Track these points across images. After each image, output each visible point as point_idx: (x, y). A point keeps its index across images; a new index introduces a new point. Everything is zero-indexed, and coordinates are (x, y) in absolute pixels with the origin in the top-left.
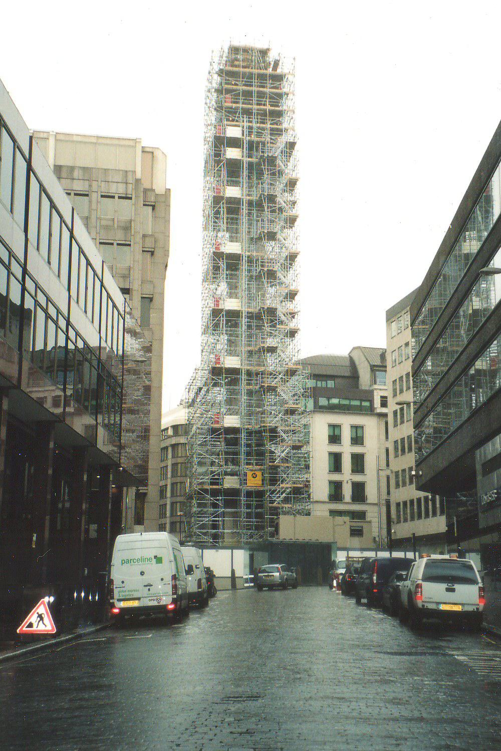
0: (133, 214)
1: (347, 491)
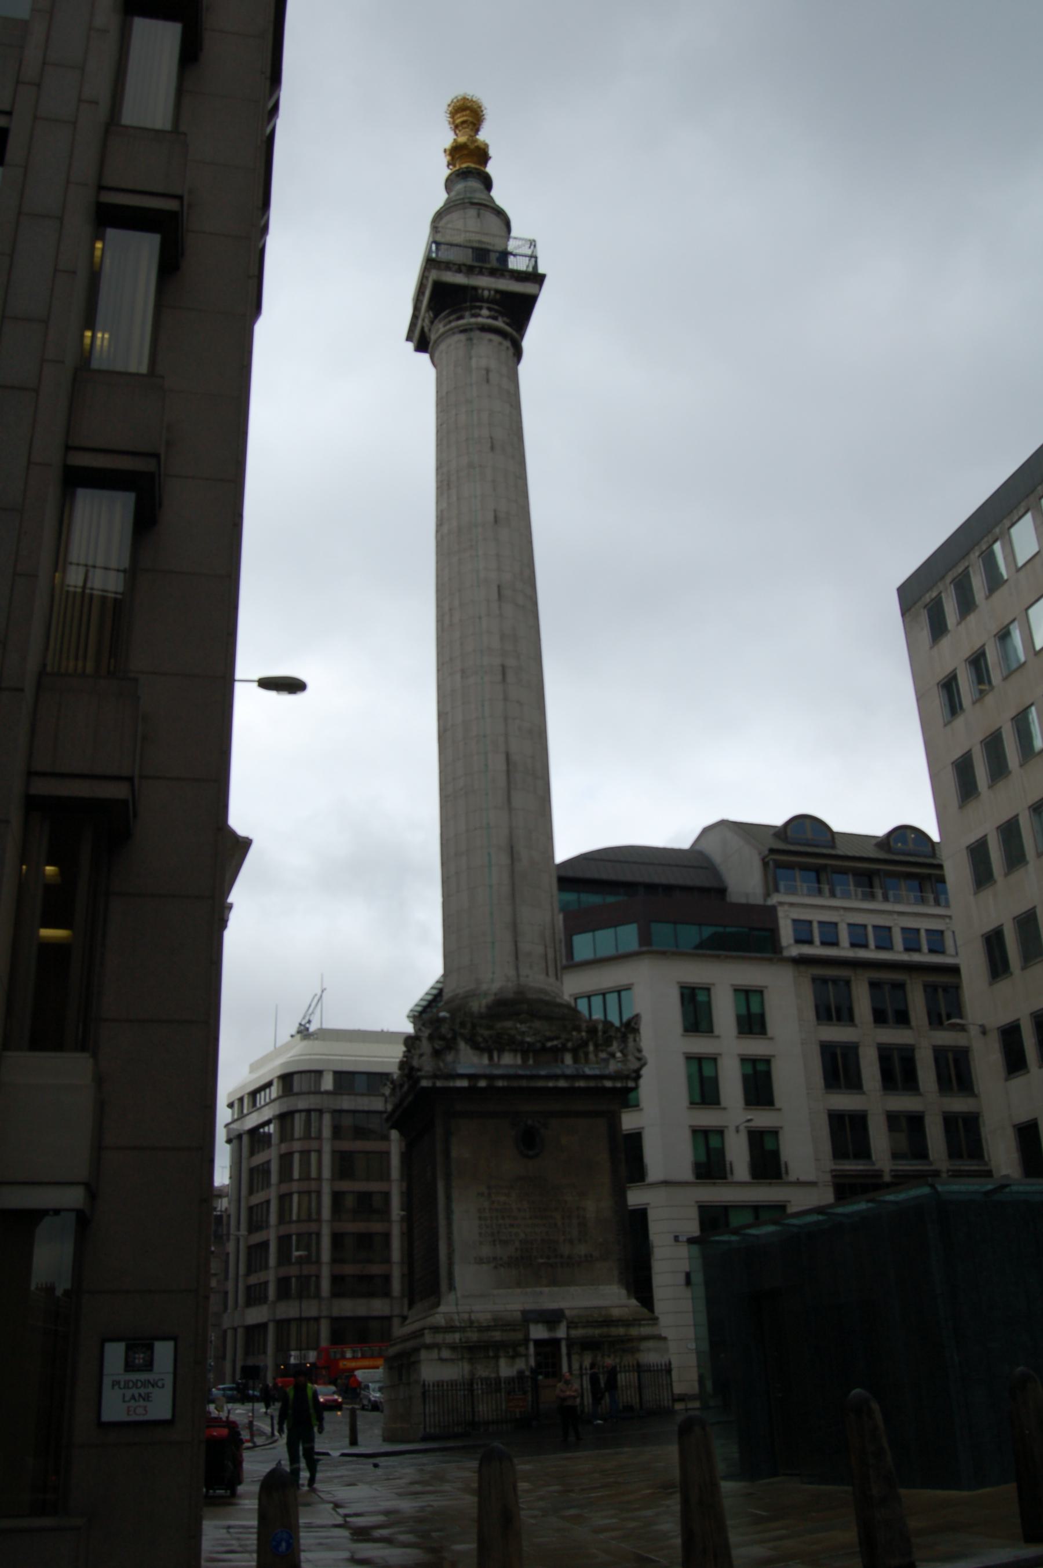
1: (738, 1153)
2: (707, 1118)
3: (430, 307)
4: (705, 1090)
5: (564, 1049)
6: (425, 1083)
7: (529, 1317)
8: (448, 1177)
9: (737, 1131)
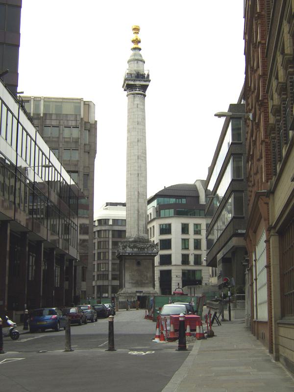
1: (192, 259)
2: (186, 252)
7: (137, 292)
8: (125, 269)
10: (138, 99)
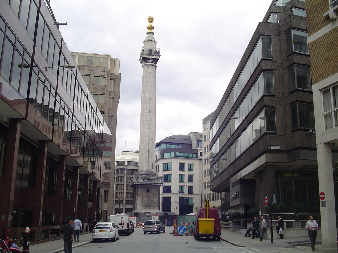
0: (106, 83)
1: (186, 190)
2: (182, 184)
3: (142, 59)
4: (182, 180)
5: (153, 179)
6: (134, 183)
8: (137, 195)
9: (186, 186)
10: (150, 69)
